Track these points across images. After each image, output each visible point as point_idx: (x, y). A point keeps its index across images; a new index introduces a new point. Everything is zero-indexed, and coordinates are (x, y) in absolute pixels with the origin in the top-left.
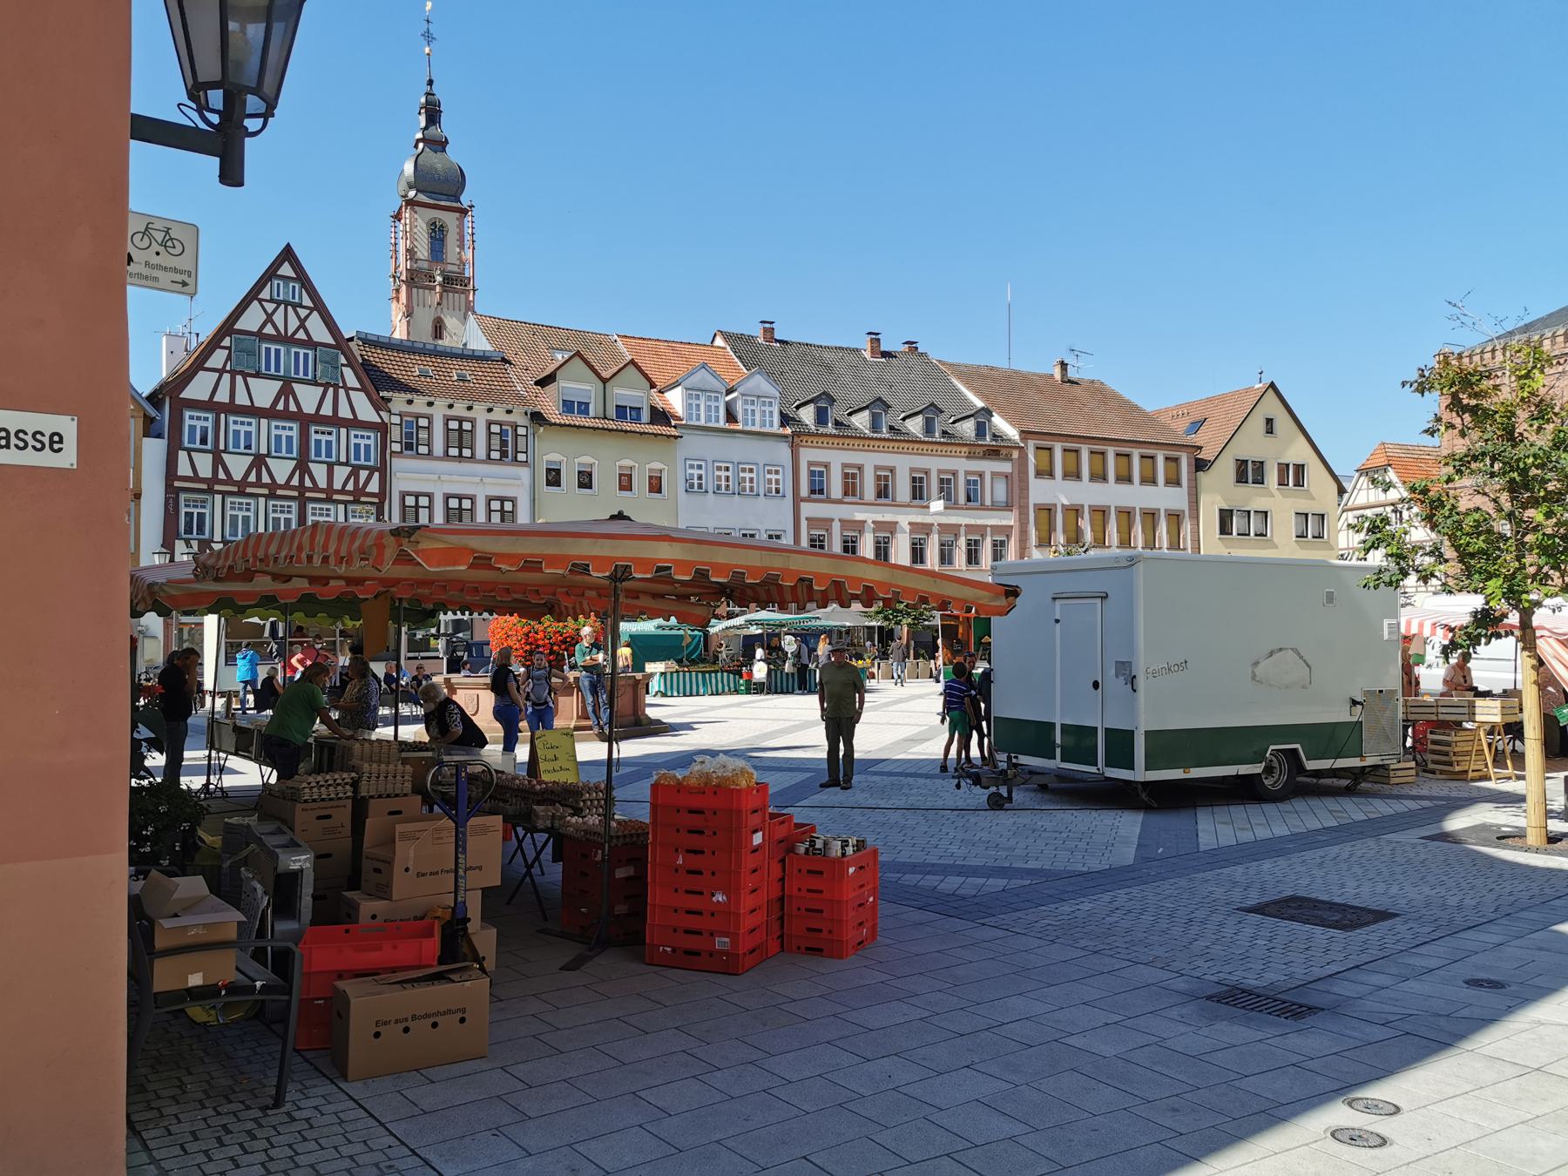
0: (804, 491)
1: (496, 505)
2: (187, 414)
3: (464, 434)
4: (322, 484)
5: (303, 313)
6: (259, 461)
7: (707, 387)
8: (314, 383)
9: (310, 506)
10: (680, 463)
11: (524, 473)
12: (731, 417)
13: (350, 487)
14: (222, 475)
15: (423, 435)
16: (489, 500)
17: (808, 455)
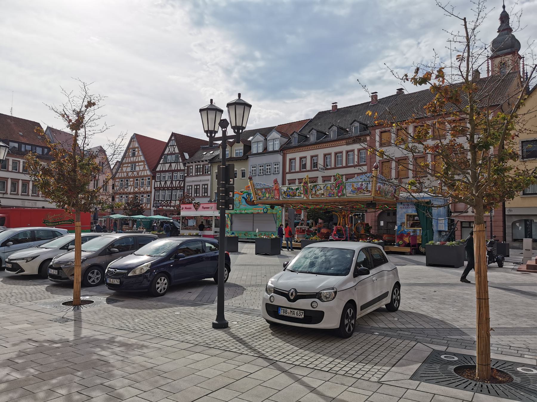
0: (287, 170)
1: (204, 186)
2: (157, 174)
3: (198, 169)
4: (174, 186)
5: (174, 147)
6: (166, 183)
7: (259, 140)
8: (174, 162)
9: (173, 191)
10: (249, 167)
11: (209, 177)
12: (265, 149)
13: (178, 186)
14: (161, 186)
15: (191, 171)
16: (195, 185)
17: (289, 156)
